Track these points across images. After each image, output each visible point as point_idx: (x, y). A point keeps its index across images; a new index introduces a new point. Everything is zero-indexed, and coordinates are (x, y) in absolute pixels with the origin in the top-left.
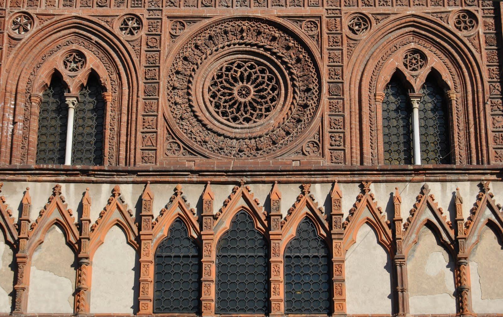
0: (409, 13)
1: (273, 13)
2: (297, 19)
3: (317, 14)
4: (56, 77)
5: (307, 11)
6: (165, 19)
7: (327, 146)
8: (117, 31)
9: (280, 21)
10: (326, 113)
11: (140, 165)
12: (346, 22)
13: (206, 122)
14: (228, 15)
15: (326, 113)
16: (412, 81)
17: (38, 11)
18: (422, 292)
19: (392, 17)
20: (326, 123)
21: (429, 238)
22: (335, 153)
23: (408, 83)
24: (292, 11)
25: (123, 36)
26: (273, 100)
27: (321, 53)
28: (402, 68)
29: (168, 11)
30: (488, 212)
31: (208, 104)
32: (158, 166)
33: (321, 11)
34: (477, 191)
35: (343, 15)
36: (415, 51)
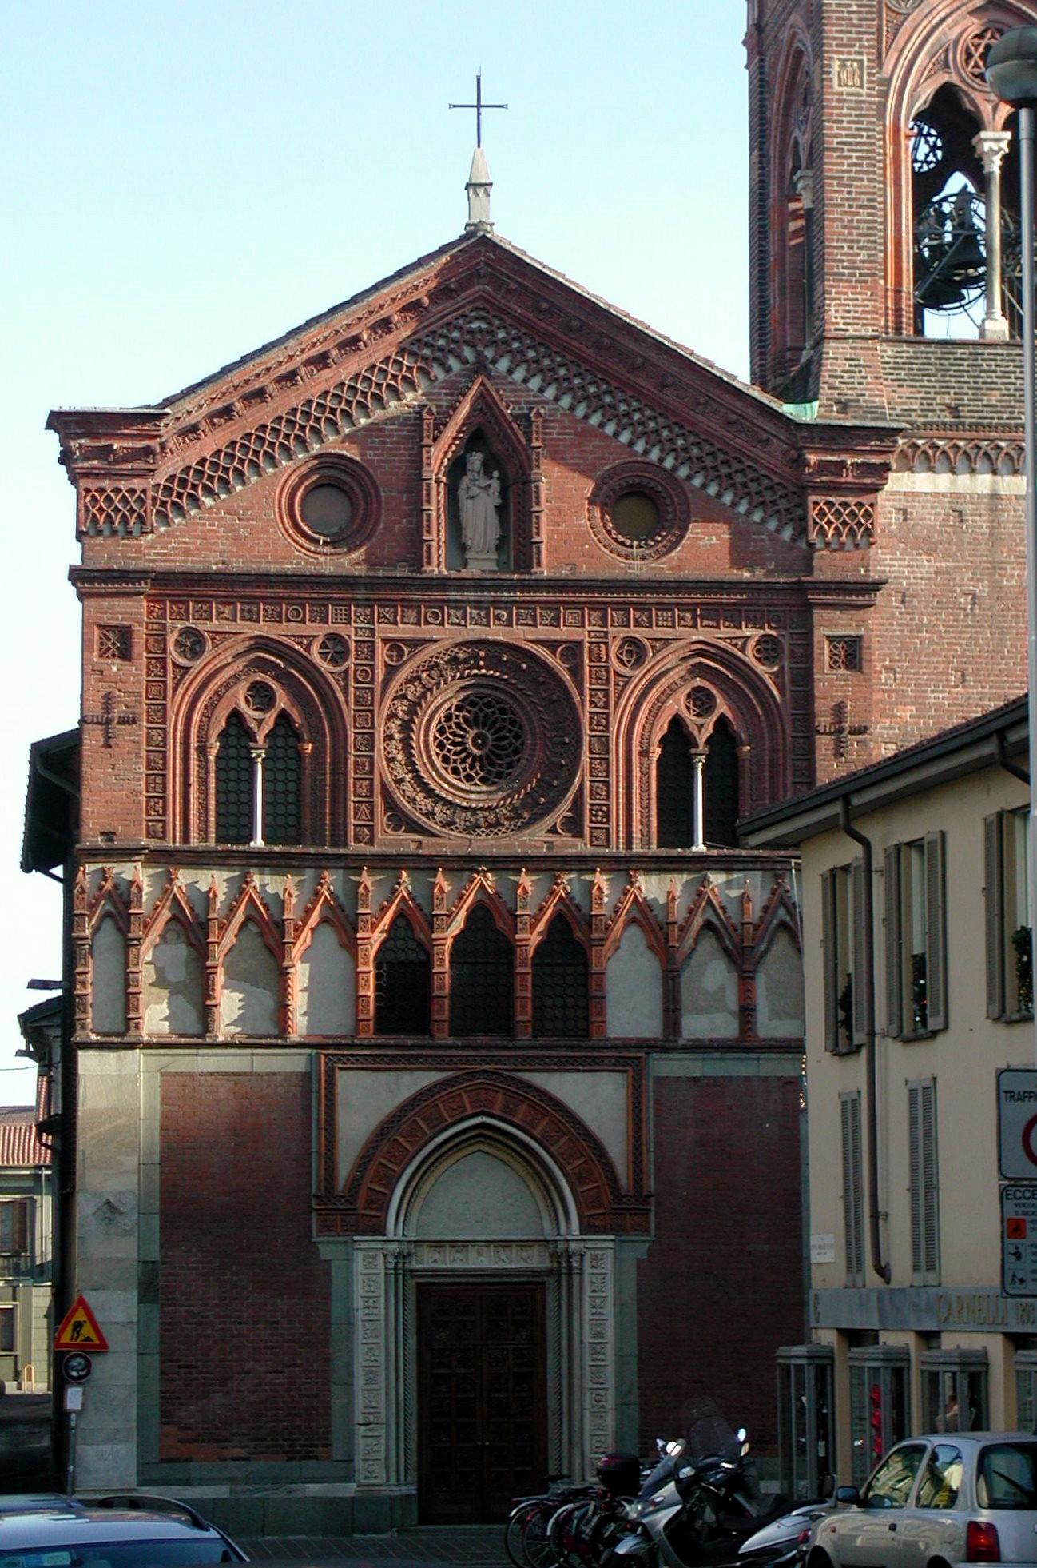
0: (695, 638)
1: (520, 634)
2: (551, 645)
3: (577, 638)
4: (236, 716)
5: (563, 633)
6: (379, 644)
7: (587, 824)
8: (316, 658)
9: (529, 647)
10: (587, 778)
11: (354, 847)
12: (614, 647)
13: (433, 785)
14: (460, 639)
15: (587, 778)
16: (696, 732)
17: (209, 626)
18: (700, 1011)
19: (675, 645)
20: (587, 792)
21: (709, 944)
22: (596, 833)
23: (691, 734)
24: (544, 632)
25: (325, 666)
26: (516, 752)
27: (581, 693)
28: (684, 712)
29: (383, 630)
30: (782, 912)
31: (434, 758)
32: (375, 849)
33: (583, 634)
34: (770, 885)
35: (610, 640)
36: (698, 690)
